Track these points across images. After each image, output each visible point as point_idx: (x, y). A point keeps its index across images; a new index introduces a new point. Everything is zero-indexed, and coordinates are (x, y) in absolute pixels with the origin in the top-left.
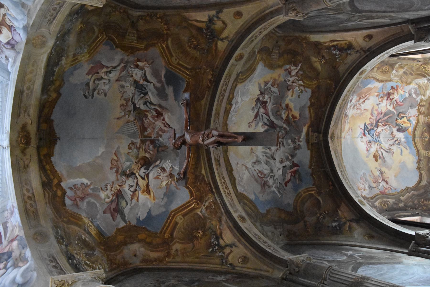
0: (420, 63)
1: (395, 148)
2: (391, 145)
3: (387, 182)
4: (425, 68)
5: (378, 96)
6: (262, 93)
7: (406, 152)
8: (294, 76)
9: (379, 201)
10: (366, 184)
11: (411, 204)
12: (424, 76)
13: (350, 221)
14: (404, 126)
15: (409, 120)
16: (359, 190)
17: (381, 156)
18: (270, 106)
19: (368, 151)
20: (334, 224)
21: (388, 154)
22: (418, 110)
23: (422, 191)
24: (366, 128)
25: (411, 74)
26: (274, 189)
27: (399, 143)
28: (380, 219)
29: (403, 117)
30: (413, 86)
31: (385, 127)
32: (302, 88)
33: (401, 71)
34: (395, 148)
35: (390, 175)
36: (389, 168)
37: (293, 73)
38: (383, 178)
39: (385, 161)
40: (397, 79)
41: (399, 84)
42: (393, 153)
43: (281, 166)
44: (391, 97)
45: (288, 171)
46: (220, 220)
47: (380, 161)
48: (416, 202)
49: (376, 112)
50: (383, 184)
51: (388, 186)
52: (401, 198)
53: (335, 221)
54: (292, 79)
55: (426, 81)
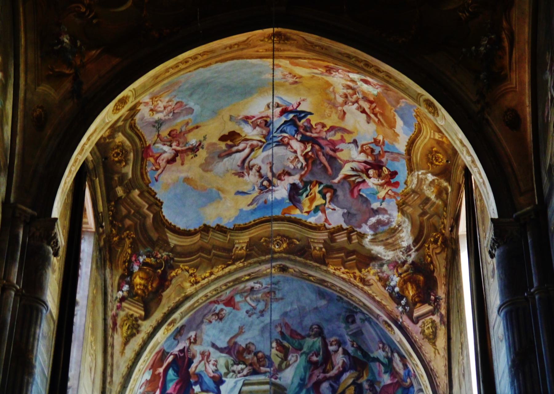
0: (447, 232)
1: (252, 178)
2: (259, 171)
3: (171, 161)
4: (436, 242)
5: (376, 142)
7: (244, 203)
9: (128, 143)
10: (168, 114)
11: (124, 211)
12: (416, 242)
14: (305, 200)
15: (317, 209)
16: (152, 99)
17: (235, 149)
19: (246, 119)
21: (239, 163)
22: (340, 229)
23: (154, 235)
24: (300, 115)
25: (424, 213)
27: (263, 189)
28: (85, 144)
29: (324, 197)
30: (396, 217)
31: (301, 159)
34: (252, 178)
36: (206, 167)
38: (182, 152)
39: (222, 156)
40: (413, 184)
41: (400, 190)
42: (240, 175)
44: (371, 172)
47: (223, 146)
49: (337, 137)
50: (168, 151)
51: (163, 163)
52: (137, 192)
53: (73, 41)
55: (405, 244)
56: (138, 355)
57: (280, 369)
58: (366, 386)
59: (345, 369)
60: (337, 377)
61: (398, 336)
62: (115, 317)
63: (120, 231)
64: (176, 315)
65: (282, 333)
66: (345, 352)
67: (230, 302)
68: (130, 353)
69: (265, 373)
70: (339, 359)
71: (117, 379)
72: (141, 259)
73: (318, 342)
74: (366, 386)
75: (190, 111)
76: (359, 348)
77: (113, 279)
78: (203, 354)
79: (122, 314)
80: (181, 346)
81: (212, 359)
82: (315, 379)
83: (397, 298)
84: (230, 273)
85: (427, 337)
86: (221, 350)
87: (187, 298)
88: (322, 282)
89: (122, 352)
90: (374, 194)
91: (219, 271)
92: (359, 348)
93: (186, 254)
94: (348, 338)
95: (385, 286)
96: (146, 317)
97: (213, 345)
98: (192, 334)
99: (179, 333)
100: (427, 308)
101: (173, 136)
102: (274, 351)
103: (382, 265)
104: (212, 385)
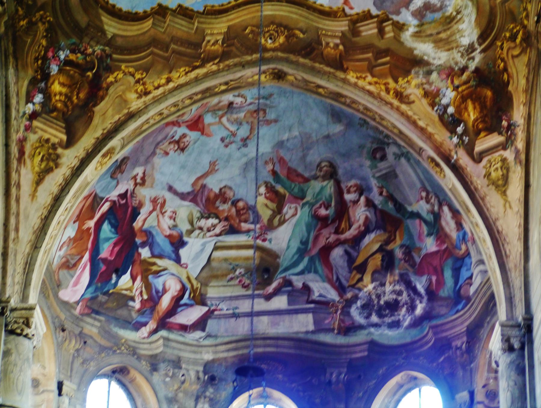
4: (513, 38)
12: (482, 37)
22: (367, 16)
23: (82, 19)
55: (465, 41)
56: (57, 200)
57: (270, 227)
58: (399, 253)
59: (367, 230)
62: (22, 142)
63: (30, 11)
64: (115, 142)
65: (274, 173)
66: (370, 203)
69: (248, 231)
73: (329, 187)
74: (399, 253)
76: (391, 197)
78: (154, 201)
79: (33, 138)
80: (121, 189)
81: (169, 209)
82: (322, 242)
84: (197, 80)
85: (494, 183)
86: (183, 196)
87: (131, 116)
88: (337, 96)
89: (33, 196)
92: (391, 197)
94: (374, 183)
95: (433, 105)
96: (70, 143)
97: (171, 189)
98: (139, 171)
100: (495, 139)
102: (262, 200)
103: (429, 73)
104: (168, 248)
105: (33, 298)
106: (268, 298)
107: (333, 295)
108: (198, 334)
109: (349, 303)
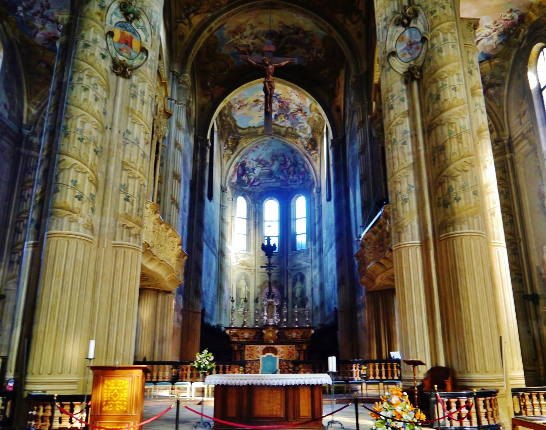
0: (321, 130)
3: (239, 109)
5: (300, 104)
6: (305, 33)
8: (316, 55)
11: (225, 123)
12: (312, 132)
13: (212, 95)
15: (283, 121)
18: (295, 37)
20: (209, 84)
22: (289, 127)
23: (234, 130)
25: (314, 124)
26: (232, 39)
30: (306, 125)
32: (308, 60)
33: (317, 119)
35: (245, 110)
37: (319, 55)
39: (254, 106)
40: (311, 116)
43: (249, 44)
45: (246, 49)
46: (208, 11)
47: (254, 103)
48: (227, 127)
49: (289, 101)
50: (238, 106)
53: (211, 84)
54: (314, 53)
56: (231, 165)
57: (272, 166)
59: (291, 166)
60: (288, 168)
61: (306, 159)
62: (223, 155)
63: (224, 130)
64: (241, 153)
66: (291, 161)
67: (257, 147)
68: (228, 164)
70: (289, 163)
71: (225, 172)
72: (231, 137)
73: (282, 158)
74: (297, 171)
75: (245, 95)
76: (295, 160)
77: (222, 143)
79: (226, 153)
83: (306, 148)
87: (244, 148)
88: (284, 142)
90: (300, 118)
91: (254, 139)
92: (295, 160)
93: (244, 135)
94: (292, 158)
96: (233, 154)
97: (252, 159)
98: (246, 157)
99: (241, 158)
100: (314, 152)
101: (239, 102)
104: (251, 170)
105: (227, 185)
106: (272, 179)
107: (284, 179)
108: (258, 187)
109: (287, 180)
